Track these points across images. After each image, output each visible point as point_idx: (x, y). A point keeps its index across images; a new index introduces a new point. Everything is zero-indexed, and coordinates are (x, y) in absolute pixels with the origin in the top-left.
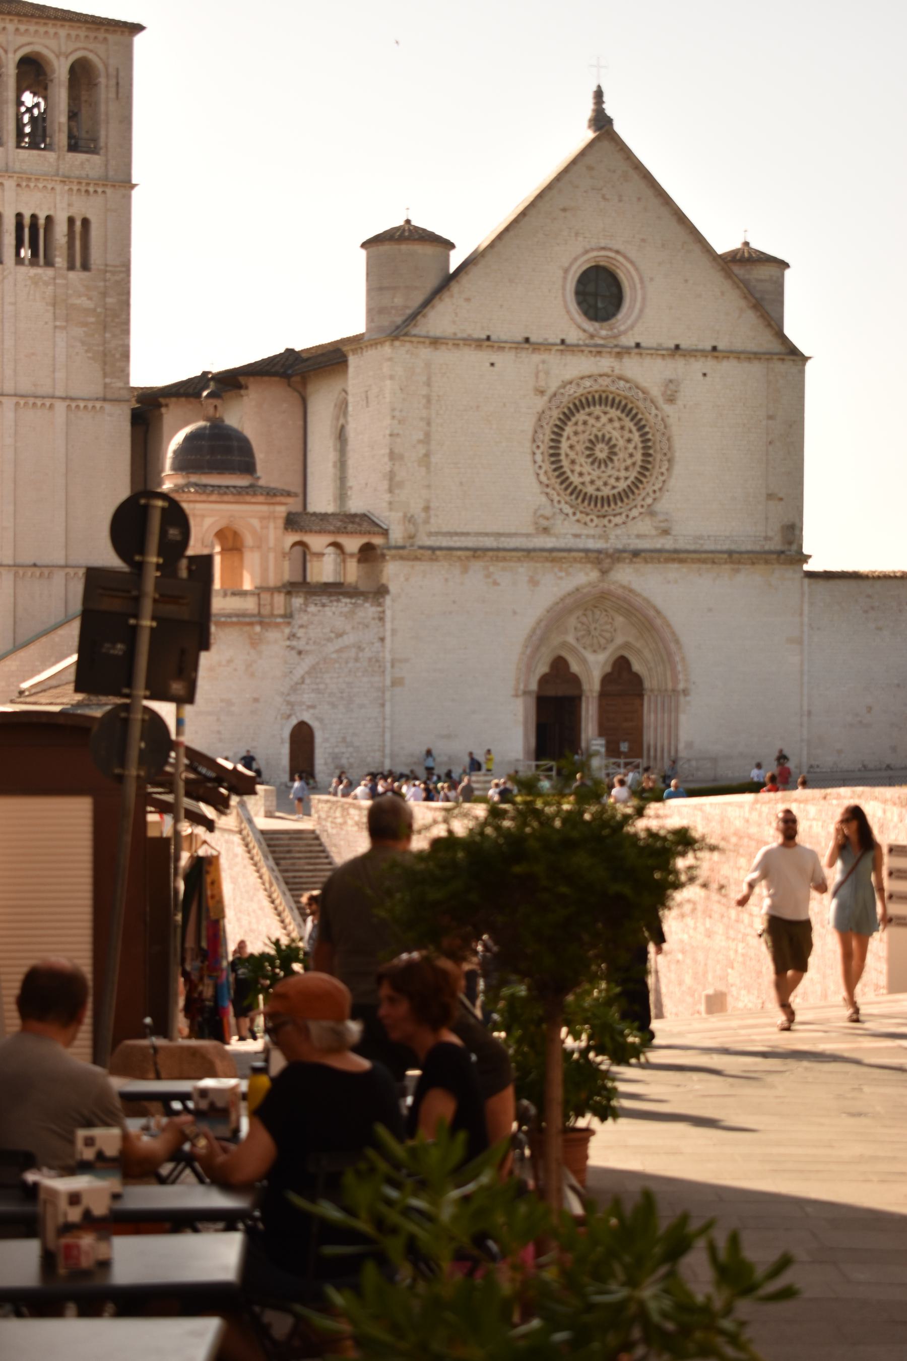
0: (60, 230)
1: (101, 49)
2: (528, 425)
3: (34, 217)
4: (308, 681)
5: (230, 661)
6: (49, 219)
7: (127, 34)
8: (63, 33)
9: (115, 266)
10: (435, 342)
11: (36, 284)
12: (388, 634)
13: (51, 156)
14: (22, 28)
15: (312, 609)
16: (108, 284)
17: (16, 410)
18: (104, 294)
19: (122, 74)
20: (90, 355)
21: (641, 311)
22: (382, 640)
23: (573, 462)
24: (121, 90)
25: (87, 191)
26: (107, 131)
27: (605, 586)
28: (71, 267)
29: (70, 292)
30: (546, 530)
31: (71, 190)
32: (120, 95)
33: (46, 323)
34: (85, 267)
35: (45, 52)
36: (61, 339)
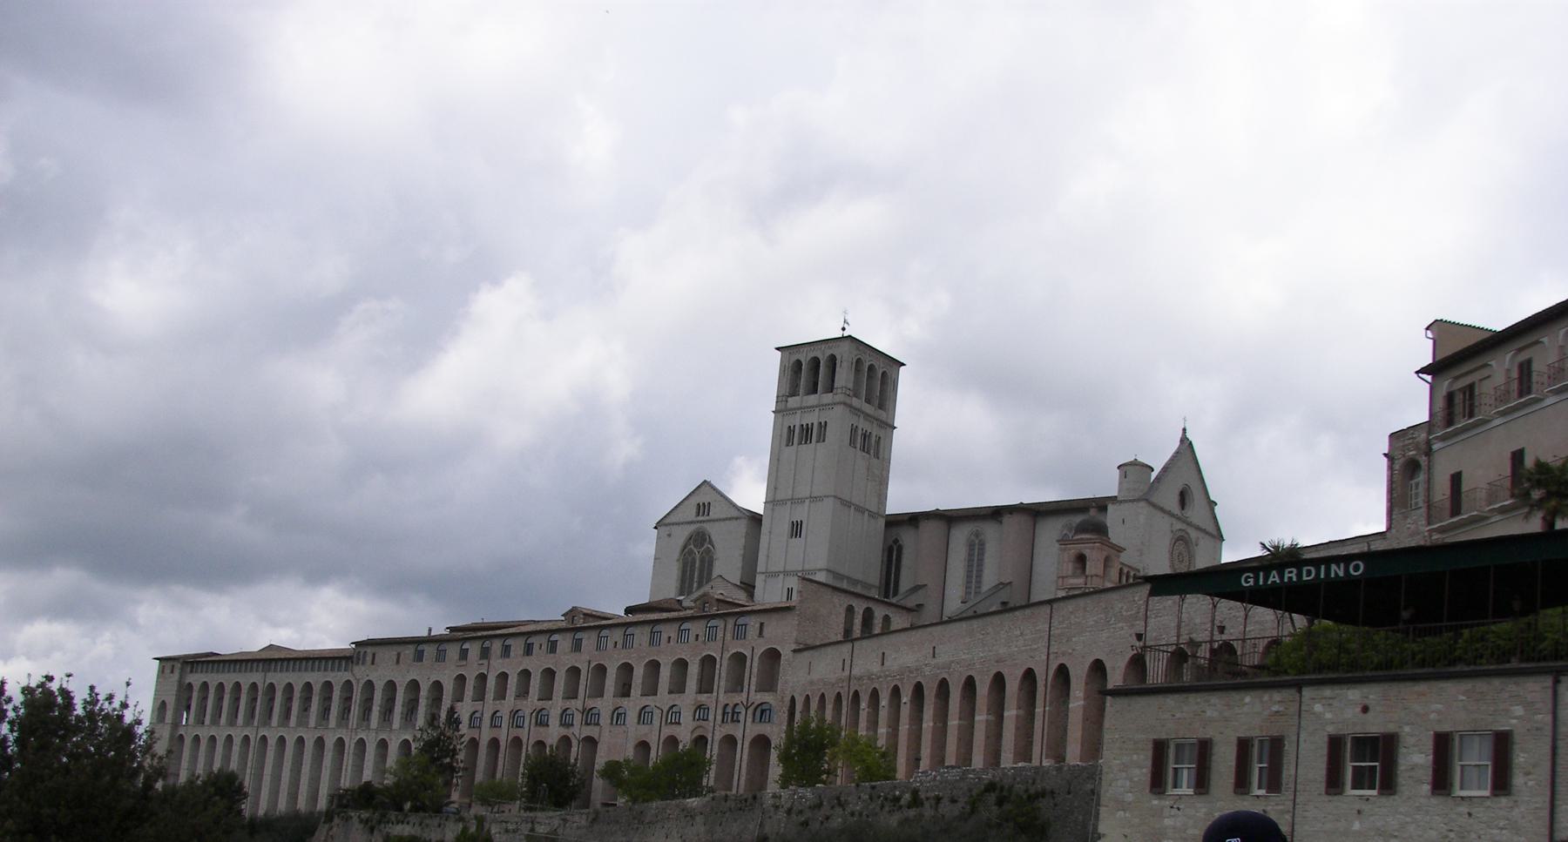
0: (873, 439)
8: (882, 360)
10: (1154, 506)
34: (878, 458)
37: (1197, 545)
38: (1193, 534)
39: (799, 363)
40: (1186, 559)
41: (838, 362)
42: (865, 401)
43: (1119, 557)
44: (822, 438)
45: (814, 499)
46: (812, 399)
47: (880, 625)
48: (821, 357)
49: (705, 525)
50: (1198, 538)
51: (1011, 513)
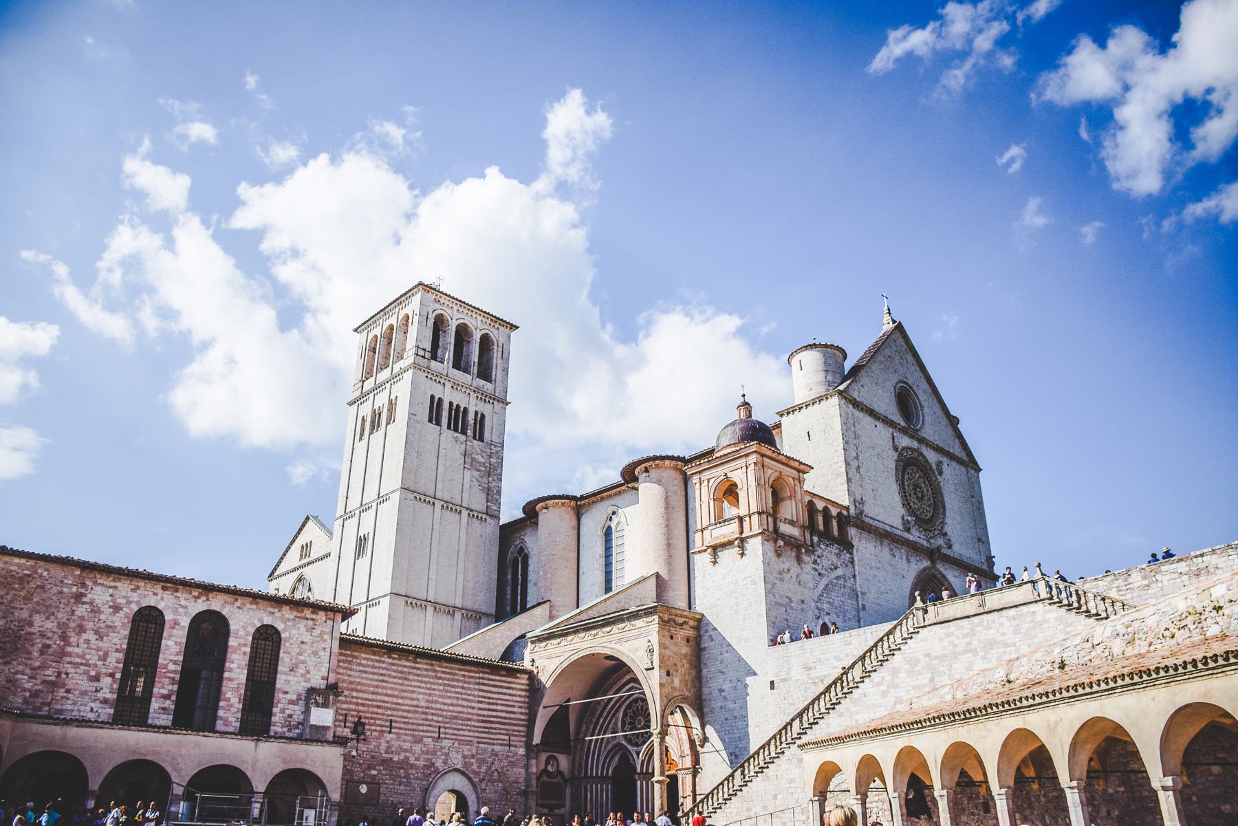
0: (471, 417)
1: (496, 332)
2: (892, 465)
3: (458, 406)
4: (825, 595)
5: (788, 570)
6: (465, 409)
8: (479, 318)
12: (857, 573)
13: (469, 377)
14: (461, 310)
15: (822, 546)
21: (923, 421)
22: (854, 576)
23: (910, 495)
25: (485, 401)
27: (933, 571)
28: (474, 438)
30: (908, 530)
31: (477, 397)
34: (481, 439)
35: (470, 325)
36: (467, 474)
37: (941, 473)
38: (932, 457)
39: (376, 337)
40: (928, 494)
41: (410, 321)
42: (457, 365)
43: (801, 481)
44: (390, 420)
45: (382, 499)
46: (385, 375)
47: (248, 650)
48: (393, 320)
49: (305, 570)
50: (939, 463)
51: (646, 470)
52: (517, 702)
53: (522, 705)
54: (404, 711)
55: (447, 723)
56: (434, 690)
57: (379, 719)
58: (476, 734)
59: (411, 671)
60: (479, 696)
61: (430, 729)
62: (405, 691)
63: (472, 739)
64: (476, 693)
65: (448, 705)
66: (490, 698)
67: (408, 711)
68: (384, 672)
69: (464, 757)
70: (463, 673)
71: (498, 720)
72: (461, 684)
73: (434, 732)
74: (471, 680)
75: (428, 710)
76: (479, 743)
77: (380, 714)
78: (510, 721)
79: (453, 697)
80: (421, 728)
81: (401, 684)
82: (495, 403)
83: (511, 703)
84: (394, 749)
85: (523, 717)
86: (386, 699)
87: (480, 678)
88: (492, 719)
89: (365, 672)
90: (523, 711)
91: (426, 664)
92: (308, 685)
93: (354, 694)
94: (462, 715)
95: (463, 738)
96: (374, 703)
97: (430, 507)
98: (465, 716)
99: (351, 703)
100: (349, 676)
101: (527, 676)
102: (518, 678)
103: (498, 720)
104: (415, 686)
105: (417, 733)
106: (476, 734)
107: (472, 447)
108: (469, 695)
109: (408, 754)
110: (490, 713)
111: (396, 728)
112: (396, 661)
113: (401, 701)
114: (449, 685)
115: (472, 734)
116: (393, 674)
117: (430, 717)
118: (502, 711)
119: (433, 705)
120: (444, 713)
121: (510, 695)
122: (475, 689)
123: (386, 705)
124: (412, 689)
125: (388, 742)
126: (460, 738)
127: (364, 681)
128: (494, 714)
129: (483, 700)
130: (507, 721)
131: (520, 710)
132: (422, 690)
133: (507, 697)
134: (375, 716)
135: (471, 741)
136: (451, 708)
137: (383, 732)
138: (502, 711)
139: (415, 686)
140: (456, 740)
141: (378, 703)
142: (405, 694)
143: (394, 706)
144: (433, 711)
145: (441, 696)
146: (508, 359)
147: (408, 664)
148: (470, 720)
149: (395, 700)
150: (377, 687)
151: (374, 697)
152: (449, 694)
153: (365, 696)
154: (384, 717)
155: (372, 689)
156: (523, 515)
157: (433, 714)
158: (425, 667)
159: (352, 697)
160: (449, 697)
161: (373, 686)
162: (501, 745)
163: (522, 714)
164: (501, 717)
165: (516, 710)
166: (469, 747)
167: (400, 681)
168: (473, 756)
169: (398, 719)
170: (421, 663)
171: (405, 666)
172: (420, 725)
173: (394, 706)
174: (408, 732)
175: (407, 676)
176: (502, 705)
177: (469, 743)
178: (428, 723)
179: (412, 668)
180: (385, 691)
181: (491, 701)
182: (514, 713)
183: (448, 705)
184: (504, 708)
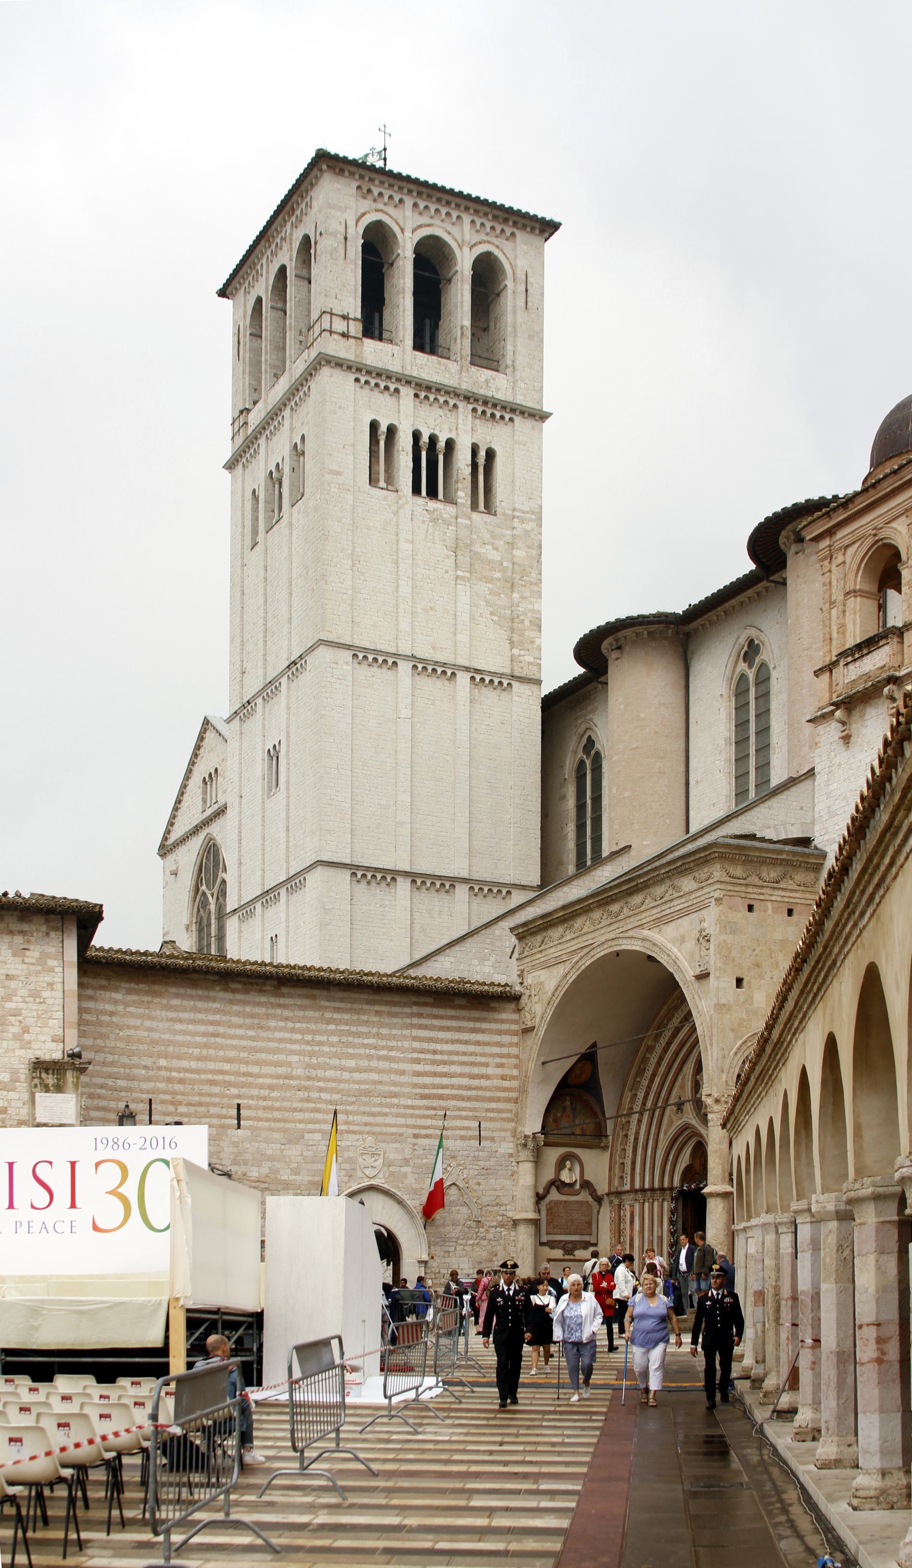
0: (463, 458)
1: (507, 246)
7: (537, 232)
9: (527, 512)
11: (434, 520)
16: (515, 532)
17: (413, 676)
18: (511, 545)
19: (530, 279)
20: (496, 618)
24: (529, 299)
25: (493, 415)
26: (515, 346)
28: (474, 506)
29: (474, 537)
32: (529, 304)
33: (447, 572)
36: (464, 593)
52: (491, 1055)
53: (503, 1060)
54: (261, 1087)
55: (351, 1104)
56: (320, 1043)
57: (215, 1105)
58: (411, 1121)
59: (271, 1011)
60: (415, 1050)
61: (319, 1116)
62: (261, 1051)
63: (403, 1130)
64: (407, 1044)
65: (352, 1070)
66: (435, 1052)
67: (271, 1088)
68: (217, 1017)
69: (388, 1164)
70: (377, 1008)
71: (454, 1092)
72: (375, 1030)
73: (324, 1122)
74: (395, 1020)
75: (309, 1083)
76: (416, 1136)
77: (215, 1095)
78: (480, 1093)
79: (360, 1055)
80: (299, 1116)
81: (251, 1038)
82: (517, 419)
83: (483, 1060)
84: (248, 1157)
85: (506, 1084)
86: (226, 1067)
87: (413, 1015)
88: (441, 1091)
89: (180, 1021)
90: (507, 1071)
91: (300, 996)
92: (31, 1055)
93: (163, 1062)
94: (379, 1087)
95: (384, 1129)
96: (203, 1077)
97: (383, 674)
98: (386, 1088)
99: (157, 1079)
100: (150, 1030)
101: (513, 1006)
102: (493, 1010)
103: (454, 1092)
104: (280, 1040)
105: (288, 1125)
106: (411, 1121)
107: (471, 528)
108: (391, 1049)
109: (278, 1165)
110: (437, 1080)
111: (249, 1118)
112: (238, 996)
113: (255, 1069)
114: (349, 1034)
115: (401, 1121)
116: (235, 1019)
117: (316, 1095)
118: (461, 1075)
119: (320, 1073)
120: (342, 1086)
121: (478, 1043)
122: (405, 1037)
123: (227, 1078)
124: (273, 1045)
125: (235, 1145)
126: (378, 1129)
127: (179, 1038)
128: (446, 1081)
129: (422, 1056)
130: (473, 1093)
131: (499, 1071)
132: (296, 1047)
133: (471, 1048)
134: (208, 1099)
135: (401, 1135)
136: (356, 1076)
137: (222, 1126)
138: (461, 1075)
139: (280, 1040)
140: (368, 1133)
141: (210, 1077)
142: (263, 1056)
143: (243, 1079)
144: (321, 1084)
145: (340, 1056)
146: (540, 309)
147: (263, 999)
148: (395, 1095)
149: (243, 1068)
150: (206, 1046)
151: (201, 1065)
152: (351, 1051)
153: (184, 1064)
154: (225, 1101)
155: (197, 1051)
156: (582, 670)
157: (321, 1090)
158: (299, 1002)
159: (160, 1068)
160: (352, 1056)
161: (197, 1045)
162: (463, 1138)
163: (503, 1078)
164: (460, 1087)
165: (490, 1071)
166: (397, 1145)
167: (251, 1033)
168: (406, 1162)
169: (251, 1102)
170: (290, 996)
171: (259, 1004)
172: (295, 1110)
173: (243, 1079)
174: (273, 1125)
175: (263, 1023)
176: (463, 1064)
177: (397, 1138)
178: (311, 1105)
179: (273, 1005)
180: (221, 1053)
181: (438, 1057)
182: (487, 1077)
183: (352, 1070)
184: (466, 1069)
